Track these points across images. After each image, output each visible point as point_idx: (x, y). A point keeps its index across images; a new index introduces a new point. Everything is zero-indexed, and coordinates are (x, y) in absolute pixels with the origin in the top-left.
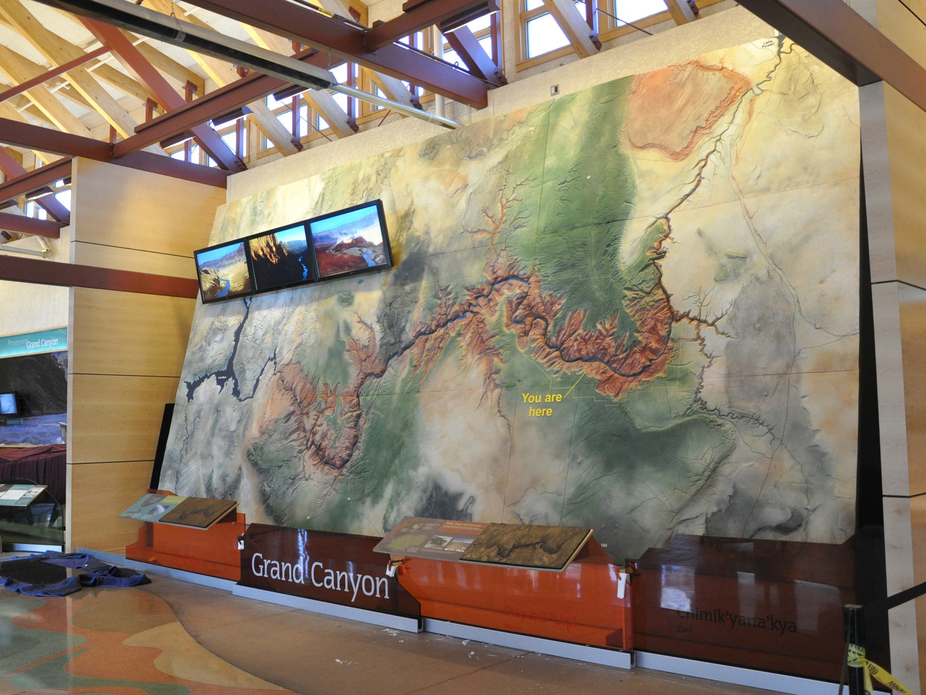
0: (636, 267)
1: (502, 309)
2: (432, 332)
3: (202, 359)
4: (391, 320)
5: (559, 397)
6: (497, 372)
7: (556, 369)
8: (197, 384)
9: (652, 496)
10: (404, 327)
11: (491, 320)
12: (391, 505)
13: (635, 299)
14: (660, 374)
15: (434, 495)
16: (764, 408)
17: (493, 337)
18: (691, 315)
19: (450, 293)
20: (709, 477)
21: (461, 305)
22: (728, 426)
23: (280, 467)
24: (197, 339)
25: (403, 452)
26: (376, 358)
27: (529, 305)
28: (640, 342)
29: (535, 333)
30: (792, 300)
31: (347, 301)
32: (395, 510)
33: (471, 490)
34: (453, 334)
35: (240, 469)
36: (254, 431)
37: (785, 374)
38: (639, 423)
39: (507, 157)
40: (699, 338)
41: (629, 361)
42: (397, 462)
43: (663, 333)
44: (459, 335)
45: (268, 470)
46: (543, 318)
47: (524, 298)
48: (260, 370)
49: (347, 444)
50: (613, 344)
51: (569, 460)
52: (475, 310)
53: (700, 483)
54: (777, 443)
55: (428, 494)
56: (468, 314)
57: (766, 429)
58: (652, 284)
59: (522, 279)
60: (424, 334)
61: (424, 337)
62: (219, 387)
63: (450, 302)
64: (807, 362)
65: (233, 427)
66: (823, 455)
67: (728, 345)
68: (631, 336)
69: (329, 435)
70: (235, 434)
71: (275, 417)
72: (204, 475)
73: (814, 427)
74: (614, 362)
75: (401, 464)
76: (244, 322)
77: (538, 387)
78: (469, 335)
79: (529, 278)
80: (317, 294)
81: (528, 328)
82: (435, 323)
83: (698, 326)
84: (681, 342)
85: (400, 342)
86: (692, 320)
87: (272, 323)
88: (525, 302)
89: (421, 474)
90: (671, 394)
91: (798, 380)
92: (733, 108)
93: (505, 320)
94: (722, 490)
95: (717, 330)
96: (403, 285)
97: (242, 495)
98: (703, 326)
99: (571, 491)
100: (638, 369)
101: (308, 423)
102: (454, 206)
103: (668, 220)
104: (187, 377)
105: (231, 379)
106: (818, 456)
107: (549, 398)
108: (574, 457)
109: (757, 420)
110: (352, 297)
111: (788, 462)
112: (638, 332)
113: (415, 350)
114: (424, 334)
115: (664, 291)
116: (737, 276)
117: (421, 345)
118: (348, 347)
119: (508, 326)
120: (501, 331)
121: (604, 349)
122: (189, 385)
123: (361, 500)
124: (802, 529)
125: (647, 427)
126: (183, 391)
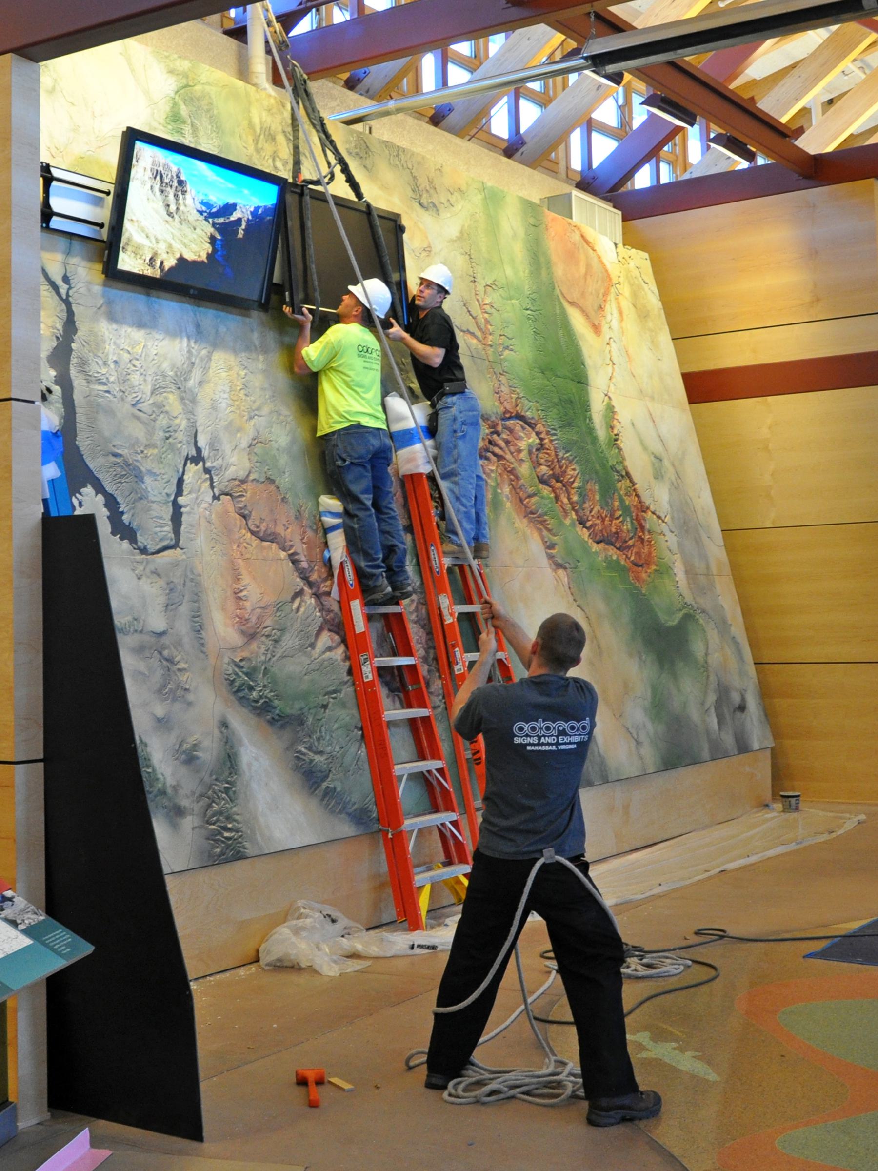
23: (325, 707)
35: (224, 724)
36: (222, 629)
38: (663, 617)
45: (300, 721)
70: (165, 640)
71: (270, 599)
97: (254, 785)
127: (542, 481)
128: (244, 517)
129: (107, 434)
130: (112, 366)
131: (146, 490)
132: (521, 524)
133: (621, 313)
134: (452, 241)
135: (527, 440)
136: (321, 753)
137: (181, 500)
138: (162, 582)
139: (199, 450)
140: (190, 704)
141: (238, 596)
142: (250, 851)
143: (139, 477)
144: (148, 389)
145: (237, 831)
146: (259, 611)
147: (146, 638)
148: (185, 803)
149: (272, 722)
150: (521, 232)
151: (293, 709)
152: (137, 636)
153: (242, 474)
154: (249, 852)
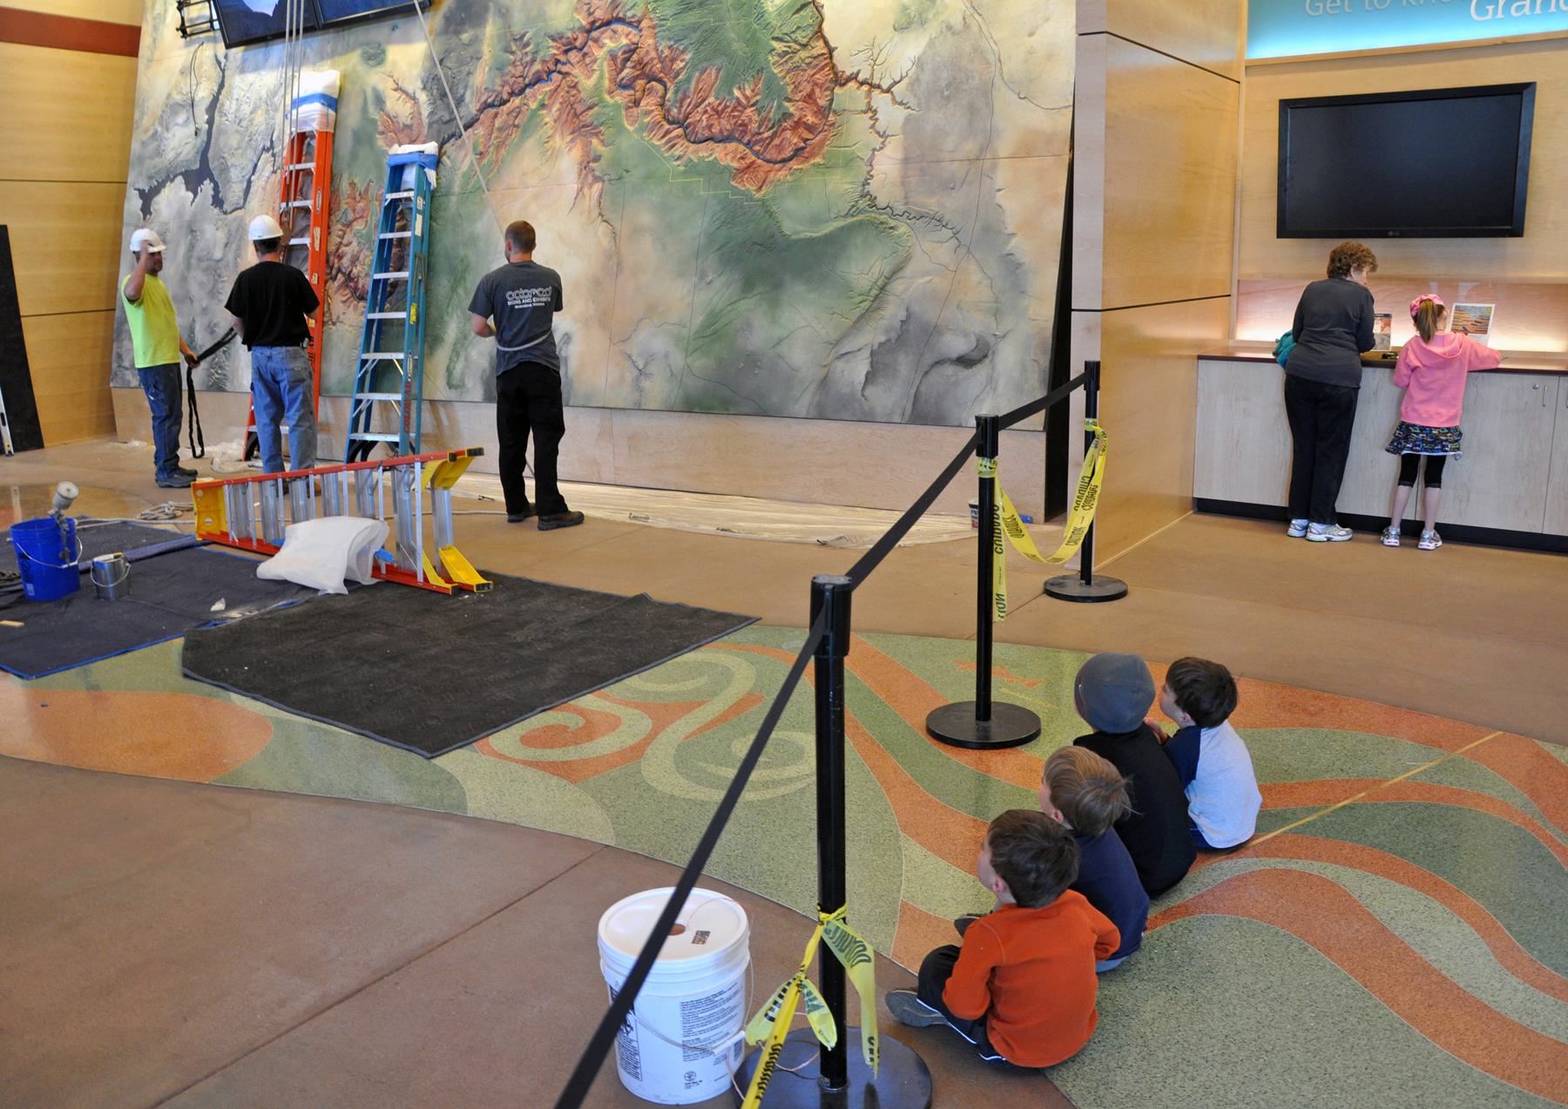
0: (789, 7)
1: (603, 68)
2: (504, 102)
3: (159, 153)
4: (442, 87)
6: (597, 159)
7: (677, 153)
8: (155, 191)
9: (803, 323)
11: (587, 83)
12: (456, 352)
13: (786, 53)
14: (818, 160)
16: (948, 204)
17: (590, 108)
18: (861, 77)
19: (527, 45)
20: (877, 297)
21: (544, 62)
22: (903, 229)
24: (146, 122)
27: (640, 62)
28: (791, 115)
29: (648, 103)
30: (992, 58)
31: (376, 57)
32: (462, 358)
34: (533, 106)
37: (978, 159)
38: (788, 227)
40: (871, 110)
41: (777, 141)
43: (822, 102)
44: (543, 106)
46: (660, 81)
47: (634, 51)
48: (250, 167)
50: (756, 118)
51: (695, 279)
52: (565, 69)
53: (865, 305)
54: (963, 250)
56: (555, 76)
57: (950, 233)
58: (809, 32)
59: (630, 24)
61: (492, 111)
62: (191, 195)
63: (528, 58)
64: (1004, 147)
65: (218, 254)
66: (1019, 265)
67: (908, 119)
68: (779, 106)
73: (1010, 230)
74: (756, 143)
76: (219, 92)
78: (557, 106)
79: (639, 22)
80: (329, 48)
81: (638, 94)
82: (507, 89)
83: (869, 92)
84: (846, 114)
86: (862, 84)
87: (264, 94)
88: (635, 57)
90: (830, 187)
91: (994, 167)
93: (606, 83)
94: (892, 313)
95: (894, 99)
96: (457, 33)
98: (876, 92)
99: (699, 320)
100: (788, 153)
104: (137, 180)
105: (207, 182)
106: (1013, 269)
108: (703, 275)
109: (940, 222)
110: (384, 52)
111: (975, 276)
112: (790, 100)
113: (480, 130)
114: (492, 105)
115: (826, 43)
116: (923, 23)
117: (487, 123)
118: (381, 128)
119: (610, 93)
120: (602, 101)
121: (744, 125)
122: (142, 193)
124: (987, 361)
125: (797, 233)
126: (134, 203)
142: (229, 387)
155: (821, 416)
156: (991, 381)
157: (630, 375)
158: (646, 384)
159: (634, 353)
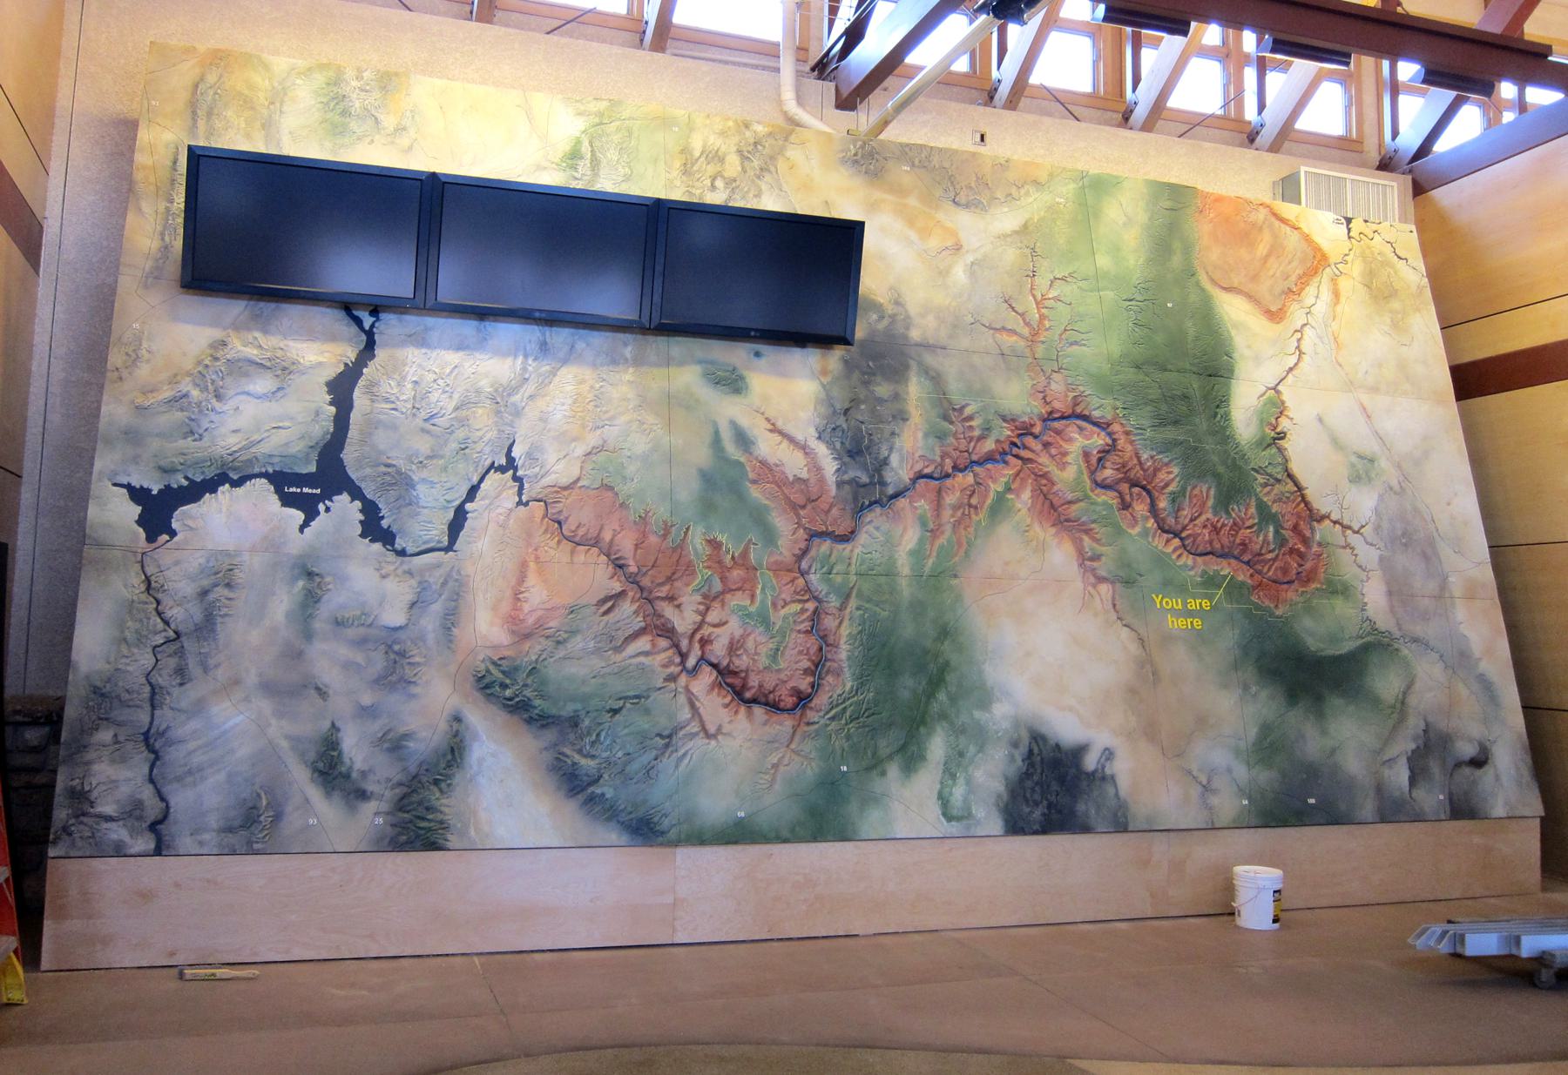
5: (1206, 604)
6: (1096, 558)
10: (886, 459)
12: (949, 773)
15: (1036, 751)
19: (970, 418)
21: (998, 441)
23: (615, 712)
25: (950, 678)
26: (832, 506)
31: (732, 383)
32: (961, 781)
33: (1100, 738)
35: (458, 719)
38: (1313, 644)
39: (1025, 226)
40: (1347, 546)
42: (942, 696)
45: (574, 722)
49: (806, 664)
52: (1024, 453)
55: (1024, 749)
57: (1437, 656)
60: (929, 476)
62: (298, 516)
63: (977, 433)
67: (1381, 559)
68: (1277, 532)
69: (750, 644)
70: (402, 635)
72: (295, 740)
74: (1259, 562)
75: (953, 699)
77: (1172, 586)
79: (1109, 425)
85: (883, 483)
89: (1000, 715)
92: (1316, 280)
94: (1414, 724)
97: (482, 780)
98: (1349, 532)
99: (1253, 732)
101: (683, 620)
102: (944, 273)
103: (1278, 392)
107: (1193, 604)
108: (1246, 688)
111: (1463, 691)
115: (1296, 483)
118: (751, 475)
120: (1087, 497)
123: (876, 765)
127: (1104, 486)
128: (559, 523)
129: (382, 447)
130: (409, 386)
131: (417, 497)
132: (1044, 532)
133: (1336, 295)
134: (1003, 237)
135: (1080, 441)
136: (593, 757)
137: (468, 506)
138: (414, 582)
139: (511, 461)
140: (413, 696)
141: (517, 597)
143: (410, 484)
144: (451, 406)
145: (442, 822)
146: (540, 613)
147: (372, 631)
148: (370, 787)
149: (530, 721)
150: (1142, 217)
151: (568, 709)
152: (362, 630)
153: (565, 481)
154: (449, 845)
155: (1383, 820)
156: (1497, 778)
157: (1195, 791)
158: (1215, 801)
159: (1194, 768)
